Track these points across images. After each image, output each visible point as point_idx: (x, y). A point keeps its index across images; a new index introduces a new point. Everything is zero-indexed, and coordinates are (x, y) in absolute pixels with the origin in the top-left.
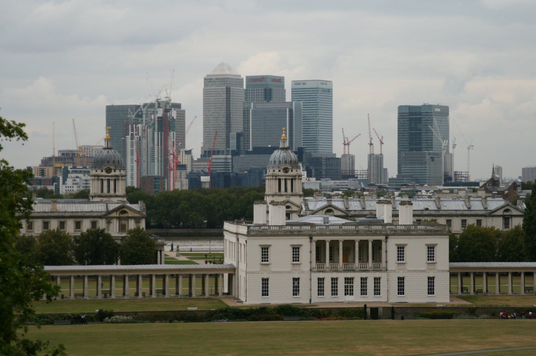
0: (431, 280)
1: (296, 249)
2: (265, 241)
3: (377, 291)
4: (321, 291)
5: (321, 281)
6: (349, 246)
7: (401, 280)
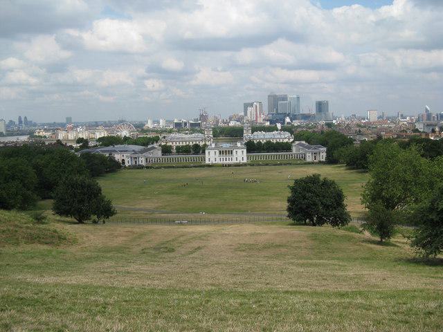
6: (226, 151)
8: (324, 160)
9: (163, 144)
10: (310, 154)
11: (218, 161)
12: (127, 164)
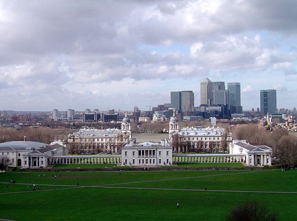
0: (168, 160)
1: (134, 152)
2: (126, 150)
3: (154, 163)
4: (140, 163)
5: (140, 160)
6: (147, 151)
7: (160, 160)
8: (270, 164)
9: (70, 141)
10: (253, 156)
11: (137, 164)
12: (25, 166)
